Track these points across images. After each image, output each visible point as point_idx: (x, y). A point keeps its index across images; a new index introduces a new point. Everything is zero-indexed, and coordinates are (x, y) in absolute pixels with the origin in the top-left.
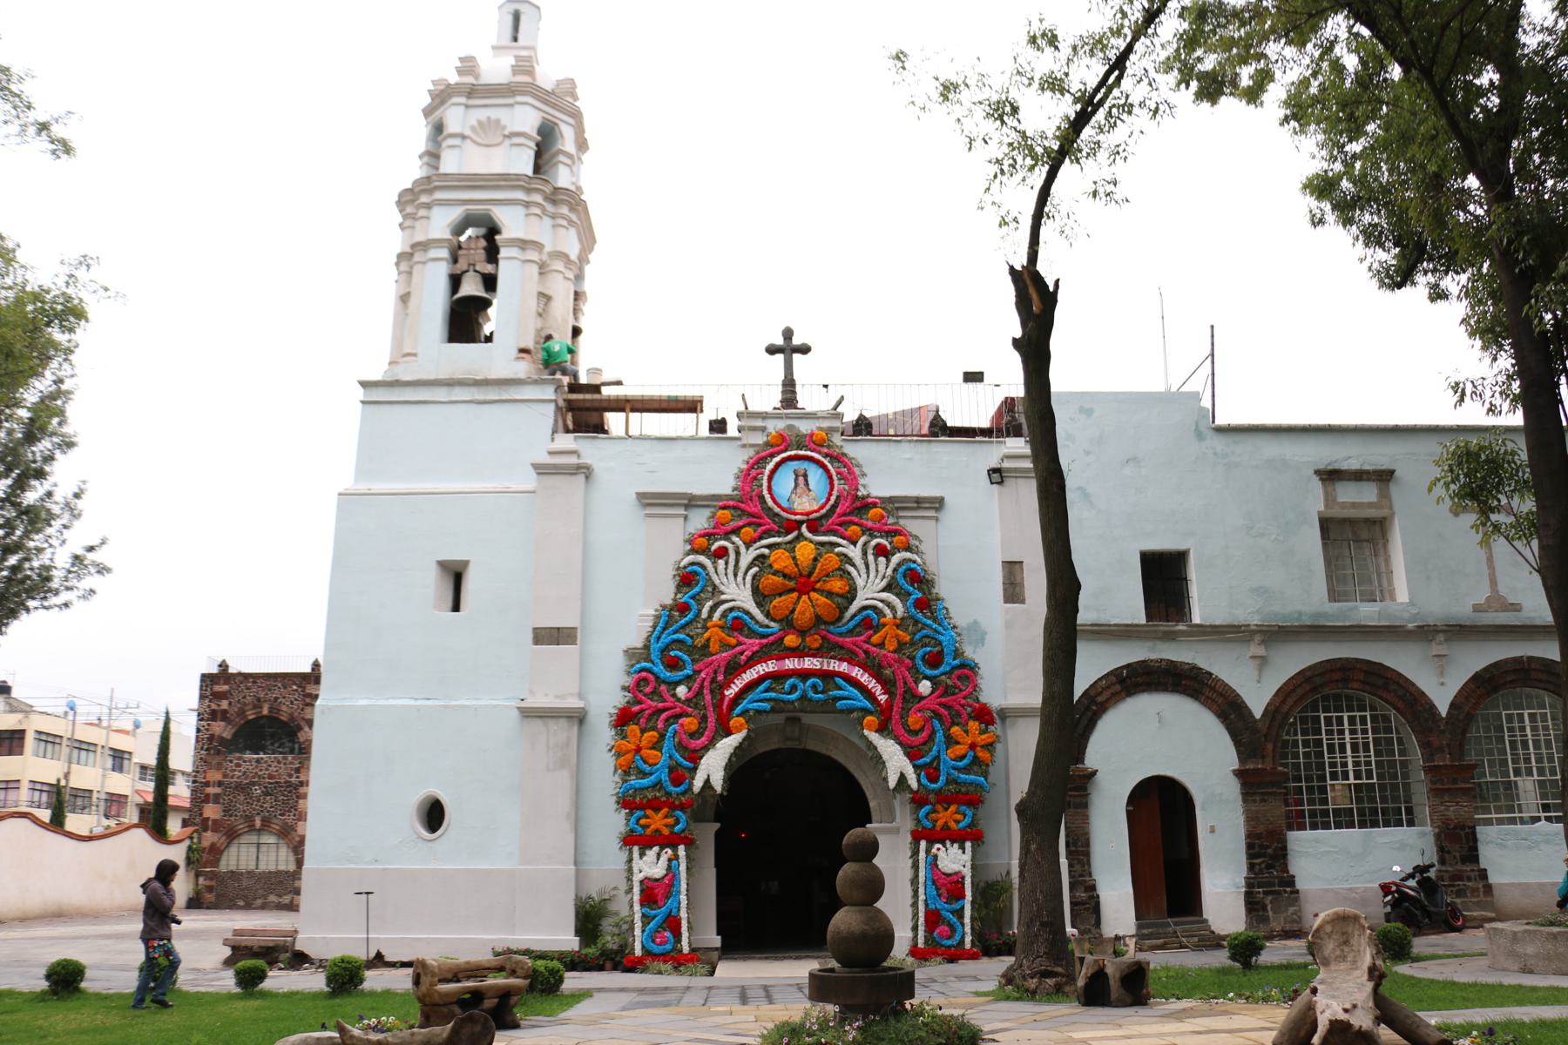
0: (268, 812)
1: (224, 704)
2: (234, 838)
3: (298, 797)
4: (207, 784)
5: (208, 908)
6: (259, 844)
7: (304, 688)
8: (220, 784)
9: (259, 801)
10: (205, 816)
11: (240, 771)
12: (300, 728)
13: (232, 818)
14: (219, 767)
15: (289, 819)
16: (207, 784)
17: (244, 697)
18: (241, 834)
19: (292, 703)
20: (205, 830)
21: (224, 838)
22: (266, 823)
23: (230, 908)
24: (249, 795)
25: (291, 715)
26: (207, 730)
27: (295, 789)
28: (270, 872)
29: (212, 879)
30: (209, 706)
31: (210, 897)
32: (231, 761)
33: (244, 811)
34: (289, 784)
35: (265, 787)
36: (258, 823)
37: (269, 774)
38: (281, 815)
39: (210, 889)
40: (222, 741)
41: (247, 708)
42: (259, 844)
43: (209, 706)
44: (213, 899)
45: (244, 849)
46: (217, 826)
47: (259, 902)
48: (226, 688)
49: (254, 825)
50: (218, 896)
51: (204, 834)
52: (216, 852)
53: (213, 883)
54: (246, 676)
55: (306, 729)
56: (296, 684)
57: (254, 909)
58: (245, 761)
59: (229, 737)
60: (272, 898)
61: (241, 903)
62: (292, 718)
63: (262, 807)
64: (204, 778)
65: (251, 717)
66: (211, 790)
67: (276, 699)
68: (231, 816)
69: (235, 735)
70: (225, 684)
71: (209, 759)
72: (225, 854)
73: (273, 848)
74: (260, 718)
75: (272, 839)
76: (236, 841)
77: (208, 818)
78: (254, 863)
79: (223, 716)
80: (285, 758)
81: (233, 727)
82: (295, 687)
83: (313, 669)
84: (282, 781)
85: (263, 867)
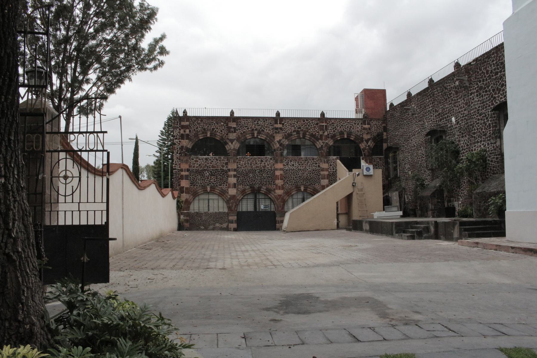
0: (213, 184)
1: (187, 131)
2: (197, 196)
3: (227, 177)
4: (182, 170)
5: (186, 230)
6: (209, 199)
7: (228, 124)
8: (188, 170)
9: (208, 178)
10: (181, 186)
11: (197, 164)
12: (226, 143)
13: (195, 187)
14: (186, 162)
15: (224, 187)
16: (182, 170)
17: (197, 128)
18: (199, 195)
19: (221, 131)
20: (182, 192)
21: (192, 196)
22: (213, 189)
23: (197, 230)
24: (203, 175)
25: (222, 137)
26: (179, 144)
27: (226, 173)
28: (216, 213)
29: (187, 216)
30: (179, 132)
31: (187, 225)
32: (193, 159)
33: (201, 183)
34: (223, 170)
35: (210, 172)
36: (209, 189)
37: (212, 165)
38: (219, 185)
39: (187, 221)
40: (187, 149)
41: (199, 133)
42: (209, 199)
43: (179, 132)
44: (188, 226)
45: (201, 202)
46: (188, 191)
47: (211, 227)
48: (187, 123)
49: (207, 190)
50: (191, 224)
51: (182, 194)
52: (188, 203)
53: (188, 218)
54: (197, 118)
55: (230, 144)
56: (223, 122)
57: (209, 230)
58: (200, 159)
59: (191, 148)
60: (217, 225)
61: (202, 227)
62: (222, 138)
63: (210, 181)
64: (180, 167)
65: (201, 138)
66: (183, 173)
67: (213, 129)
68: (194, 186)
69: (193, 147)
70: (186, 121)
71: (182, 158)
72: (192, 204)
73: (216, 202)
74: (206, 139)
75: (215, 197)
76: (197, 198)
77: (183, 187)
78: (207, 208)
79: (188, 137)
80: (221, 158)
81: (192, 142)
82: (222, 124)
83: (231, 115)
84: (219, 169)
85: (211, 211)
